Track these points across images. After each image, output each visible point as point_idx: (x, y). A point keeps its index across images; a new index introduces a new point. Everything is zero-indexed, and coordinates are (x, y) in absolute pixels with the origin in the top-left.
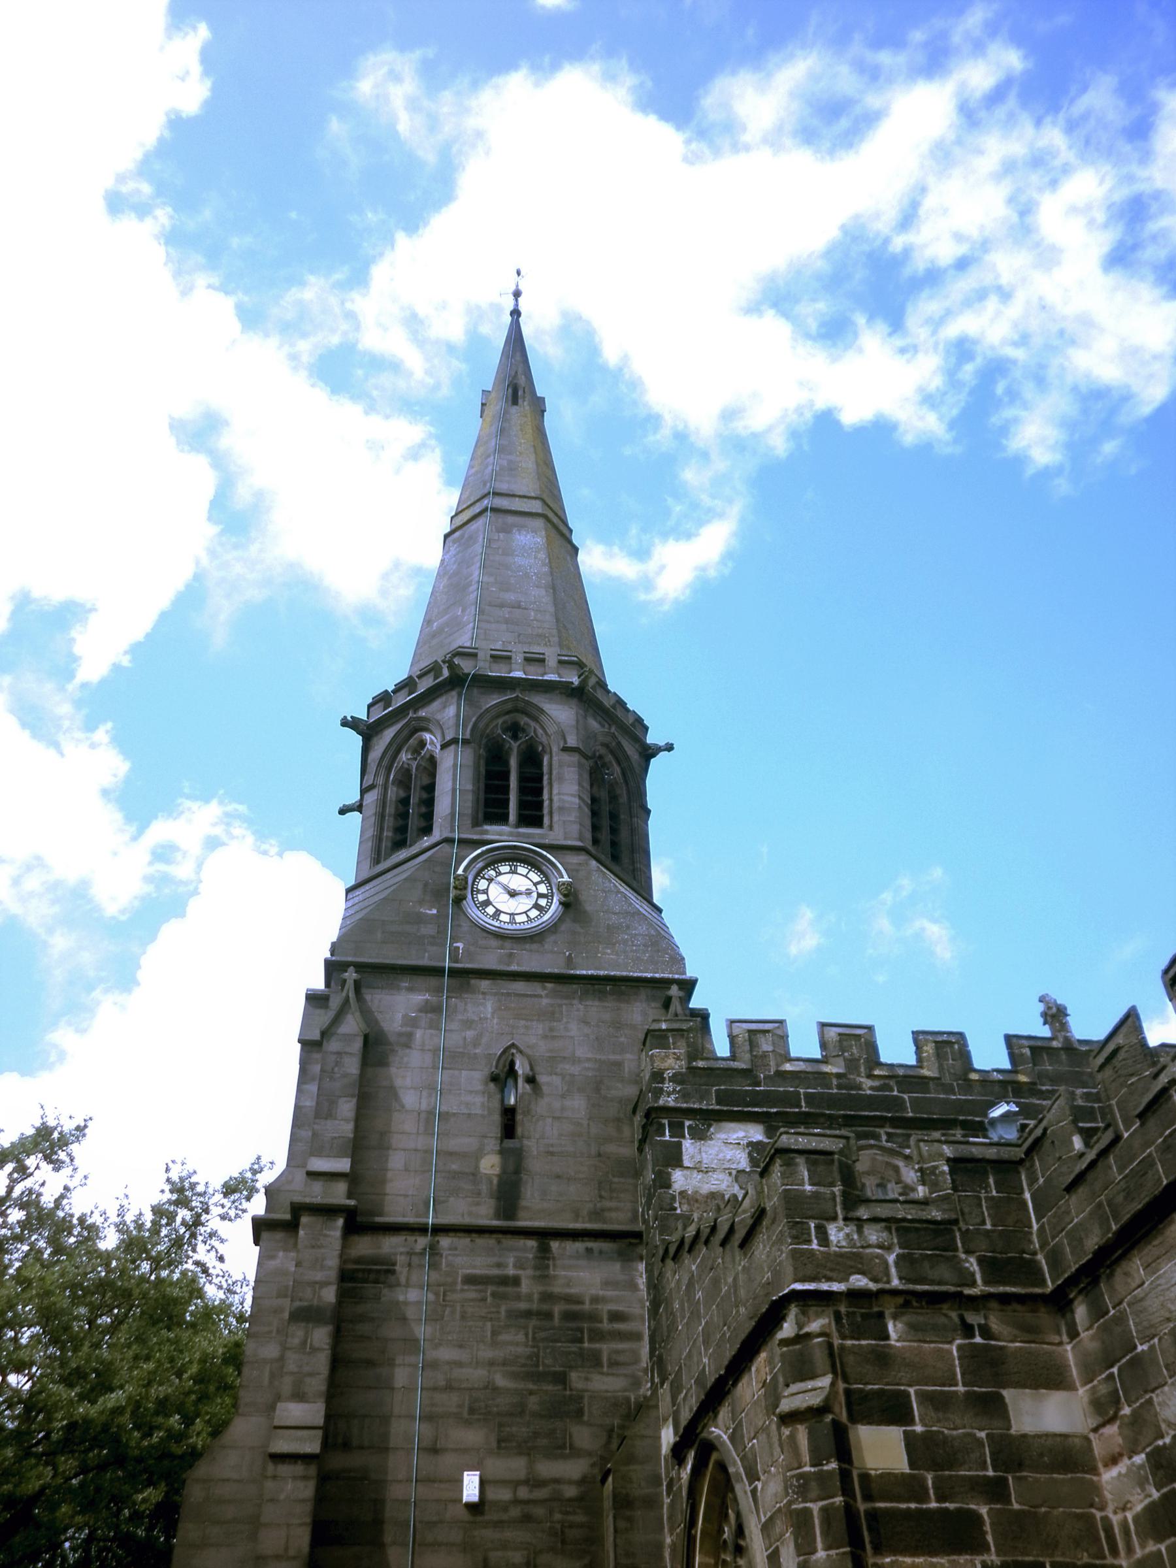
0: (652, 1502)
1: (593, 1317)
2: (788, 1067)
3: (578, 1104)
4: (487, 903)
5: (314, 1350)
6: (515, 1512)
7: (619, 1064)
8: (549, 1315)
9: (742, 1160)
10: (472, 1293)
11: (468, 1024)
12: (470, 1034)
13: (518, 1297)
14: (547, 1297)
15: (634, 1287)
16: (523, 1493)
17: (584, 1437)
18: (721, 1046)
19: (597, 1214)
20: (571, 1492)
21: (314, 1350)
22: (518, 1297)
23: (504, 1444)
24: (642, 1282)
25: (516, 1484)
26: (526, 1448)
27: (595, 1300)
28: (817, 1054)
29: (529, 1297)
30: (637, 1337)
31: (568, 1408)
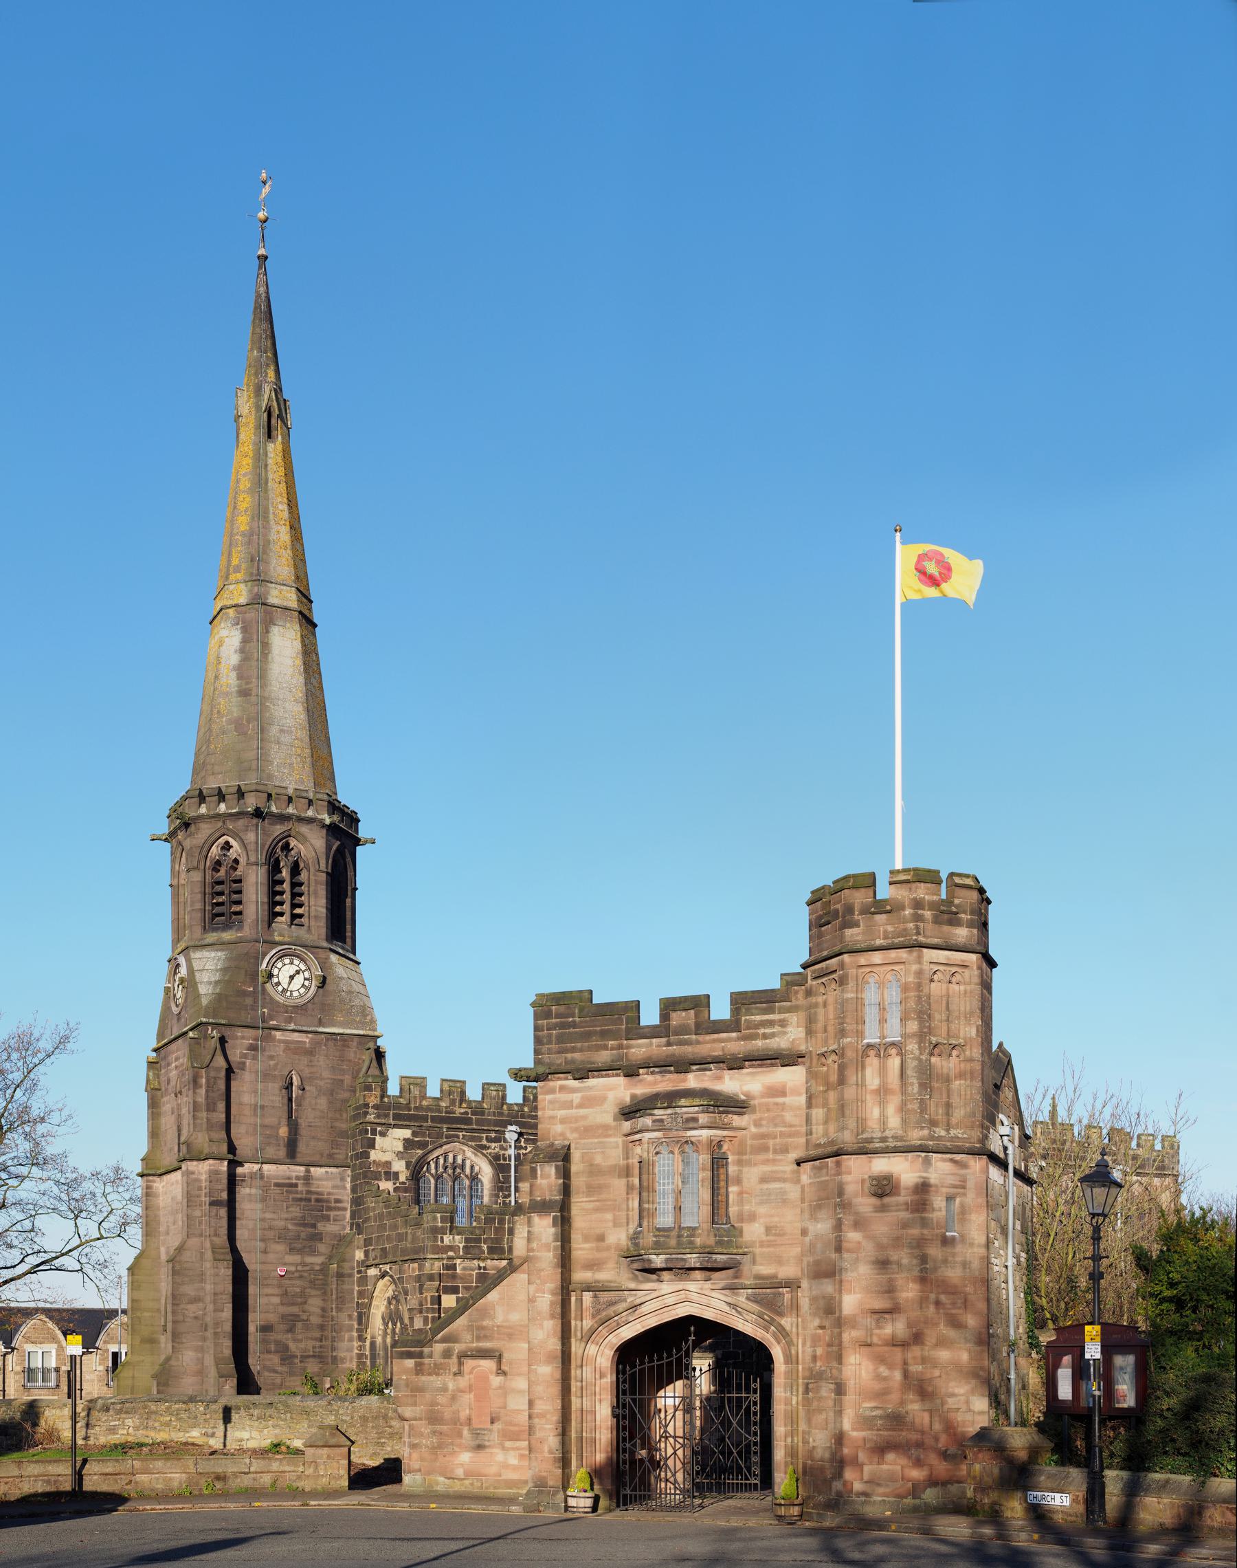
0: (351, 1275)
1: (328, 1201)
2: (425, 1103)
3: (323, 1102)
4: (278, 984)
5: (221, 1218)
6: (296, 1274)
7: (342, 1081)
8: (310, 1200)
9: (401, 1149)
10: (278, 1190)
11: (271, 1057)
12: (272, 1063)
13: (297, 1192)
14: (309, 1192)
15: (345, 1188)
16: (299, 1268)
17: (322, 1248)
18: (393, 1089)
19: (331, 1156)
20: (317, 1268)
21: (221, 1218)
22: (297, 1192)
23: (292, 1250)
24: (348, 1186)
25: (297, 1265)
26: (300, 1251)
27: (329, 1194)
28: (438, 1095)
29: (301, 1192)
30: (345, 1209)
31: (317, 1237)
